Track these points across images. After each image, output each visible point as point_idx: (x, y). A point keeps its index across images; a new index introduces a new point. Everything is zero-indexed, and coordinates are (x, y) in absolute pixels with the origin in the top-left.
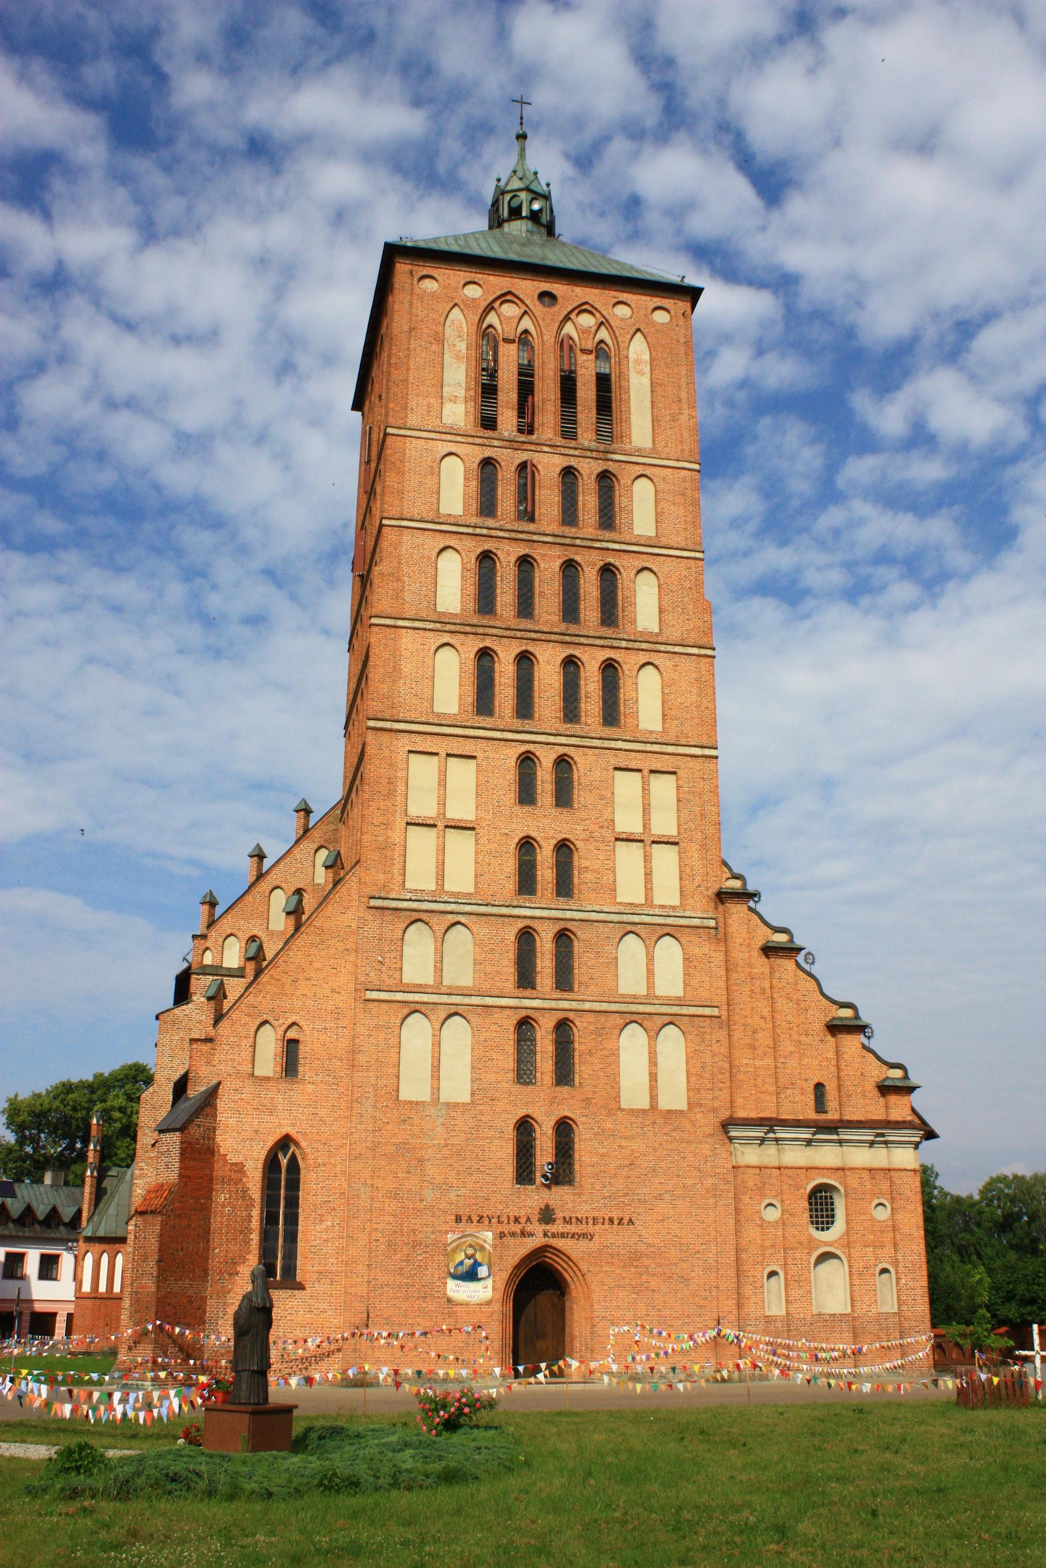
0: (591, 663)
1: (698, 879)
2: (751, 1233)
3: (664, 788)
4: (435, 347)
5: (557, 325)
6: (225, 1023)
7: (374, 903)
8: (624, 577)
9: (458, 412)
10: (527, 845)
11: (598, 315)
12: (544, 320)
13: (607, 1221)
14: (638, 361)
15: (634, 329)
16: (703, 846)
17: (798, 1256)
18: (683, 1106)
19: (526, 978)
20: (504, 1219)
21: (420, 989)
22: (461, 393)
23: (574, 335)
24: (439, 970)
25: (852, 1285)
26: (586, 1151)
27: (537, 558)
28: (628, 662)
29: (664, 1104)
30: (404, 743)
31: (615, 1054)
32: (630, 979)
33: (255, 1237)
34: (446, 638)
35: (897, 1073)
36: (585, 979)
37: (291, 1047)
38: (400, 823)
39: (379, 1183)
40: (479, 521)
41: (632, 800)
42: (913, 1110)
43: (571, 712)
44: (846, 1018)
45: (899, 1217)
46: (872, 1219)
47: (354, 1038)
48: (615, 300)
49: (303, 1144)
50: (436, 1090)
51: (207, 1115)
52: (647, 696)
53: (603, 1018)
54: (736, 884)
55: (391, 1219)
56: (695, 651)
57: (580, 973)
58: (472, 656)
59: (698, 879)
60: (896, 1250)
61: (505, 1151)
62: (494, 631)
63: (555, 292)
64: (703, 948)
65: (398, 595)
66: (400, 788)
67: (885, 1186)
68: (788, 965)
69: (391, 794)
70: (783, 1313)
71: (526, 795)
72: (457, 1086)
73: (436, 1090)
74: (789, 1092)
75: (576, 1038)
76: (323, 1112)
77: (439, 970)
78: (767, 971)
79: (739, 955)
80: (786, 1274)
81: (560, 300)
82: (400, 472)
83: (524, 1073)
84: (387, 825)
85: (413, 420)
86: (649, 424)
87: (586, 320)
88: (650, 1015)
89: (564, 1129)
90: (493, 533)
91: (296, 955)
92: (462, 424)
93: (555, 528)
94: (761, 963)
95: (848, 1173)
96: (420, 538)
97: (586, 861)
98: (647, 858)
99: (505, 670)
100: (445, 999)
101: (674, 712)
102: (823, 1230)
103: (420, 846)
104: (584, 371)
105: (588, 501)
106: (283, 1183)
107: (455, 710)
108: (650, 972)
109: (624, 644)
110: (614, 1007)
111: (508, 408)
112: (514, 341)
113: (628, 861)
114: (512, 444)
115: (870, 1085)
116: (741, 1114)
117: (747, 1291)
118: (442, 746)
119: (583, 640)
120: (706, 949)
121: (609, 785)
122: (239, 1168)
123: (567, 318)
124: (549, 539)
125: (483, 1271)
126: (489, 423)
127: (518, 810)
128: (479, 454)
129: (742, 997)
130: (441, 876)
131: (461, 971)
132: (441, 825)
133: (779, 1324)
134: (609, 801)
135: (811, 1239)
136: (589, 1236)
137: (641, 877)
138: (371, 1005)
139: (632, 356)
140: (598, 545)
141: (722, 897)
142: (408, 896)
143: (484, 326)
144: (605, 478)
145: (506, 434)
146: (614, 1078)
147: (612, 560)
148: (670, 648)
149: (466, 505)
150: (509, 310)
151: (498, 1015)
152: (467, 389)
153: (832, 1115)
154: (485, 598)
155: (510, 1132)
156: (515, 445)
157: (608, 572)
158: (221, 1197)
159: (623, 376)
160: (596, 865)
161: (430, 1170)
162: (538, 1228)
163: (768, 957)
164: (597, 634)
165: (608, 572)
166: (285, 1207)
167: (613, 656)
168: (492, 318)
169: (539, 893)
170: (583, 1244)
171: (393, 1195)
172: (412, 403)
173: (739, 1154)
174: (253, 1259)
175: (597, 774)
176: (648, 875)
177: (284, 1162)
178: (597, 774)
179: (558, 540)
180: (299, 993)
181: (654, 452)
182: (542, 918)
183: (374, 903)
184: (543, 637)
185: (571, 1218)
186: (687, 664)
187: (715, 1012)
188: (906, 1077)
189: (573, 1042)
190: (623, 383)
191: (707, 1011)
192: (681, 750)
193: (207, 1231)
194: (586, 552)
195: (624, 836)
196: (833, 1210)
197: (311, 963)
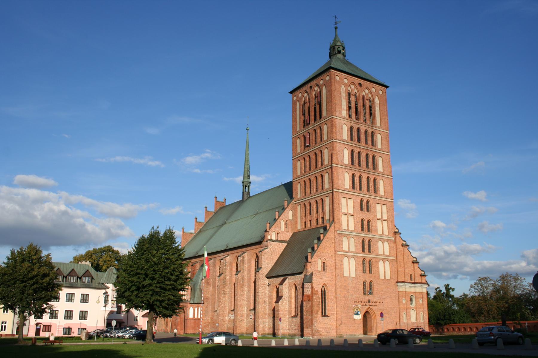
2: (401, 305)
7: (338, 232)
9: (345, 113)
10: (362, 221)
21: (346, 252)
26: (375, 287)
30: (340, 195)
31: (378, 267)
33: (321, 306)
50: (350, 274)
54: (397, 230)
64: (392, 245)
65: (337, 159)
72: (353, 274)
73: (350, 274)
83: (364, 272)
84: (339, 214)
96: (341, 145)
97: (372, 224)
100: (350, 254)
103: (344, 218)
105: (369, 138)
107: (348, 188)
116: (399, 280)
117: (401, 317)
118: (347, 196)
121: (375, 207)
122: (317, 291)
125: (359, 313)
126: (350, 116)
129: (399, 255)
134: (375, 210)
136: (375, 305)
137: (381, 228)
141: (395, 233)
144: (373, 133)
146: (378, 272)
153: (413, 281)
157: (374, 157)
159: (374, 107)
161: (350, 292)
162: (367, 304)
165: (374, 157)
174: (321, 311)
175: (374, 205)
178: (374, 205)
183: (338, 232)
186: (388, 180)
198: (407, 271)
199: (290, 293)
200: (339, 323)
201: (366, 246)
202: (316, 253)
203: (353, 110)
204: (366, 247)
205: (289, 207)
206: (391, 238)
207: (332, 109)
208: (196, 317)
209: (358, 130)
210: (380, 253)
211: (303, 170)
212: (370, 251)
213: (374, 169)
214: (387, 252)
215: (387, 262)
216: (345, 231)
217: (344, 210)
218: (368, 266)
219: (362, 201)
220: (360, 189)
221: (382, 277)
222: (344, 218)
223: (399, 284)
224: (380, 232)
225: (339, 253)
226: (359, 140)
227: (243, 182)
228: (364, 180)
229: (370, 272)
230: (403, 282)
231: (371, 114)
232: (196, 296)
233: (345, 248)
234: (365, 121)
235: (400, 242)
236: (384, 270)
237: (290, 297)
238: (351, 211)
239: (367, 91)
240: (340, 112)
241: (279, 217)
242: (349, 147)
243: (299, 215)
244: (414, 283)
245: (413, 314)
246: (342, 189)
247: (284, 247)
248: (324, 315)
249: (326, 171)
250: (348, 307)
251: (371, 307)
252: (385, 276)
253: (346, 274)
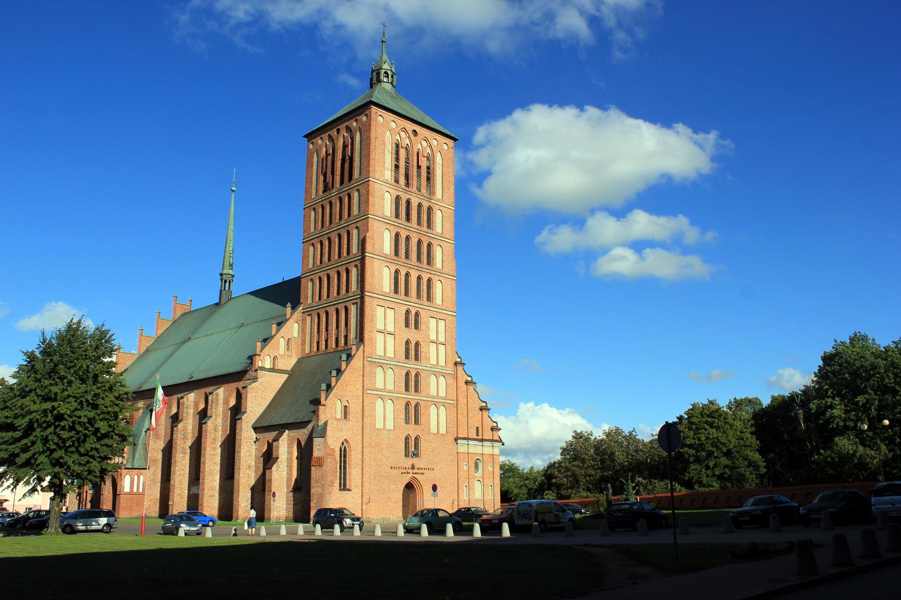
2: (461, 473)
9: (388, 175)
10: (408, 342)
26: (423, 446)
28: (435, 279)
30: (376, 302)
31: (429, 415)
54: (459, 360)
64: (452, 381)
65: (373, 246)
72: (390, 425)
82: (373, 197)
83: (407, 421)
97: (423, 348)
116: (460, 436)
117: (460, 492)
122: (333, 450)
126: (397, 181)
128: (395, 193)
129: (460, 398)
134: (428, 328)
136: (423, 474)
137: (436, 356)
141: (456, 364)
146: (429, 422)
153: (480, 437)
157: (429, 245)
162: (411, 471)
186: (449, 282)
198: (471, 421)
199: (290, 453)
200: (365, 500)
201: (412, 382)
202: (334, 391)
203: (402, 170)
204: (412, 384)
205: (294, 316)
207: (369, 166)
208: (135, 490)
209: (408, 202)
211: (319, 260)
212: (416, 390)
213: (429, 263)
214: (442, 393)
215: (442, 409)
218: (413, 414)
219: (408, 312)
220: (407, 294)
221: (434, 430)
222: (380, 337)
223: (459, 441)
224: (433, 361)
225: (369, 392)
226: (408, 219)
227: (221, 275)
229: (416, 422)
230: (464, 439)
231: (428, 179)
232: (137, 456)
233: (379, 384)
234: (419, 189)
235: (462, 377)
236: (437, 419)
237: (290, 460)
238: (390, 328)
239: (424, 144)
240: (382, 173)
241: (277, 332)
242: (392, 228)
243: (308, 330)
244: (482, 440)
245: (478, 486)
247: (284, 380)
248: (344, 487)
249: (354, 264)
250: (381, 476)
251: (415, 476)
252: (438, 429)
253: (379, 425)
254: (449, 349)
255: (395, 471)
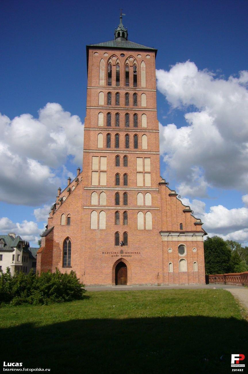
0: (131, 135)
1: (155, 180)
2: (166, 255)
3: (148, 161)
4: (98, 68)
5: (124, 61)
6: (55, 214)
7: (85, 188)
8: (139, 116)
9: (103, 82)
10: (117, 174)
11: (134, 58)
12: (122, 60)
13: (134, 253)
14: (143, 68)
15: (142, 60)
16: (156, 174)
17: (176, 260)
18: (151, 229)
19: (117, 203)
20: (113, 253)
22: (104, 78)
23: (129, 63)
24: (99, 202)
25: (188, 266)
27: (120, 113)
28: (140, 134)
29: (147, 228)
30: (92, 154)
32: (140, 202)
33: (62, 257)
34: (100, 132)
35: (199, 221)
36: (130, 203)
37: (68, 219)
38: (91, 171)
39: (87, 246)
40: (107, 106)
41: (142, 164)
42: (202, 228)
43: (127, 146)
44: (187, 209)
45: (199, 251)
46: (192, 252)
47: (81, 216)
48: (138, 54)
49: (71, 239)
50: (98, 226)
51: (51, 233)
52: (144, 142)
53: (134, 211)
54: (163, 181)
55: (89, 253)
56: (155, 131)
57: (129, 201)
58: (106, 135)
59: (155, 180)
60: (198, 258)
61: (113, 239)
62: (111, 130)
63: (124, 54)
64: (155, 195)
66: (91, 164)
67: (196, 245)
68: (174, 198)
69: (89, 165)
70: (172, 272)
71: (117, 164)
72: (103, 226)
74: (174, 225)
75: (128, 215)
76: (75, 232)
77: (99, 202)
78: (170, 200)
79: (164, 197)
80: (173, 264)
81: (125, 55)
85: (93, 85)
86: (145, 82)
87: (131, 59)
88: (145, 210)
89: (125, 234)
90: (110, 108)
91: (69, 200)
92: (104, 85)
93: (124, 106)
94: (169, 198)
95: (187, 242)
97: (130, 178)
98: (144, 176)
99: (113, 137)
100: (100, 208)
101: (150, 145)
102: (182, 254)
104: (131, 71)
105: (131, 100)
106: (68, 246)
108: (144, 201)
109: (139, 130)
110: (136, 208)
111: (114, 80)
112: (115, 65)
113: (140, 177)
114: (114, 88)
115: (193, 223)
117: (165, 267)
118: (99, 155)
119: (130, 130)
120: (156, 195)
123: (127, 59)
124: (123, 109)
126: (109, 84)
127: (116, 168)
130: (99, 182)
131: (103, 202)
132: (99, 171)
133: (171, 274)
134: (136, 165)
135: (178, 256)
138: (85, 210)
139: (141, 66)
140: (133, 109)
141: (160, 184)
142: (92, 187)
143: (109, 62)
145: (113, 86)
147: (136, 113)
148: (149, 131)
149: (105, 103)
150: (114, 58)
151: (111, 211)
152: (105, 77)
153: (184, 230)
154: (108, 123)
155: (114, 235)
156: (115, 89)
158: (55, 250)
160: (133, 178)
161: (97, 243)
162: (119, 255)
163: (170, 196)
164: (133, 129)
166: (68, 251)
167: (136, 133)
168: (110, 61)
169: (120, 185)
170: (129, 258)
171: (90, 248)
172: (93, 81)
173: (163, 239)
174: (61, 262)
175: (133, 159)
176: (144, 180)
177: (68, 242)
179: (124, 109)
180: (70, 208)
181: (146, 88)
182: (121, 190)
183: (85, 188)
184: (121, 130)
185: (127, 252)
186: (152, 134)
187: (158, 209)
188: (201, 222)
189: (127, 216)
190: (140, 73)
191: (156, 209)
192: (152, 153)
193: (52, 256)
194: (131, 111)
195: (139, 172)
196: (184, 250)
197: (72, 201)
204: (121, 200)
206: (155, 188)
210: (139, 204)
216: (95, 187)
217: (95, 167)
222: (95, 176)
225: (85, 207)
228: (122, 138)
236: (144, 221)
238: (104, 167)
244: (183, 233)
246: (93, 149)
252: (145, 227)
253: (94, 226)
254: (154, 175)
255: (106, 255)
